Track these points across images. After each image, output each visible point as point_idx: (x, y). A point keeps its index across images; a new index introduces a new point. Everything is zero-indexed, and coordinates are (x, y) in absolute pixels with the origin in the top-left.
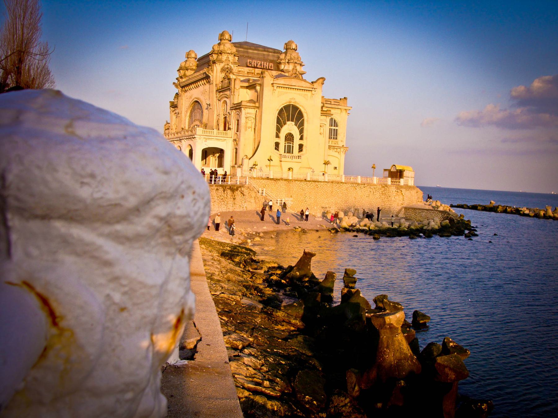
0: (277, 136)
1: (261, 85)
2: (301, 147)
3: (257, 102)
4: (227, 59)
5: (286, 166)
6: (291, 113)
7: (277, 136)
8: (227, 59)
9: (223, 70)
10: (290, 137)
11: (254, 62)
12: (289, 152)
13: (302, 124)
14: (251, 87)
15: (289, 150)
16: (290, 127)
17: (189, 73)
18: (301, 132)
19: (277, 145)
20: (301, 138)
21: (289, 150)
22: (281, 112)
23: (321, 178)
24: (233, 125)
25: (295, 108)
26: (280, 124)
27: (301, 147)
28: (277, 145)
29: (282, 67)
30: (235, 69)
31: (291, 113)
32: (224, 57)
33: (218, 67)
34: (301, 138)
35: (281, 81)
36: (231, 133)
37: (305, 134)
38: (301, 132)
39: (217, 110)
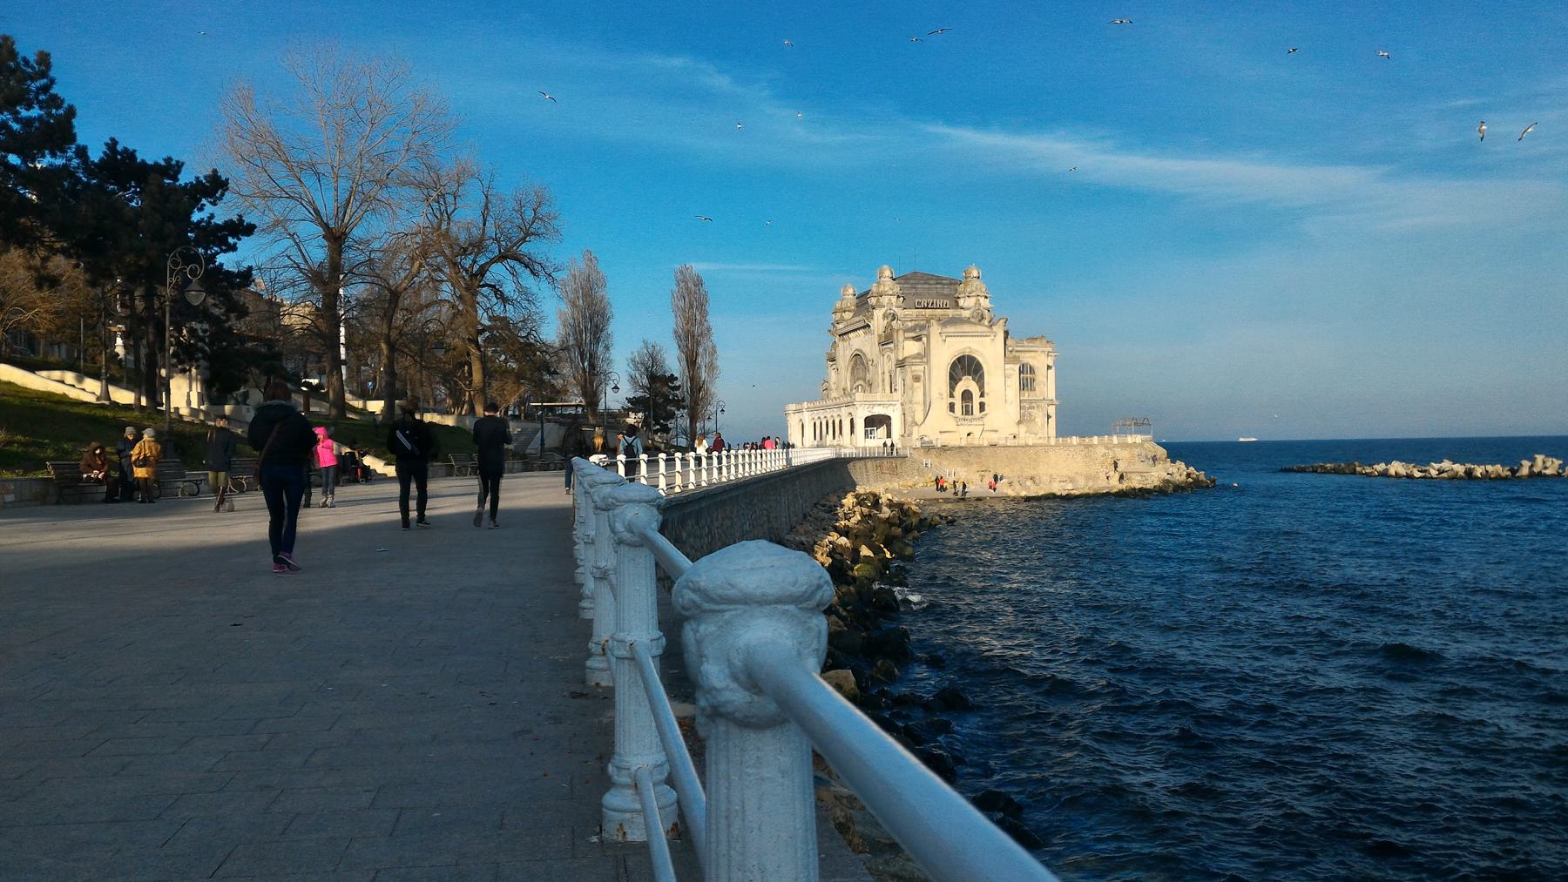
0: (951, 396)
1: (928, 337)
2: (982, 406)
3: (924, 356)
4: (890, 302)
5: (965, 430)
6: (966, 366)
7: (951, 396)
8: (890, 302)
9: (885, 316)
10: (967, 396)
11: (924, 302)
12: (967, 413)
13: (982, 377)
14: (918, 339)
15: (967, 411)
16: (967, 383)
17: (847, 315)
18: (981, 387)
19: (952, 407)
20: (982, 395)
21: (967, 411)
22: (953, 366)
23: (1011, 442)
24: (899, 387)
25: (972, 359)
26: (954, 380)
27: (982, 406)
28: (952, 407)
29: (961, 302)
30: (899, 312)
31: (966, 366)
32: (885, 300)
33: (878, 313)
34: (982, 395)
35: (951, 329)
36: (897, 396)
37: (986, 389)
38: (981, 387)
39: (883, 365)
